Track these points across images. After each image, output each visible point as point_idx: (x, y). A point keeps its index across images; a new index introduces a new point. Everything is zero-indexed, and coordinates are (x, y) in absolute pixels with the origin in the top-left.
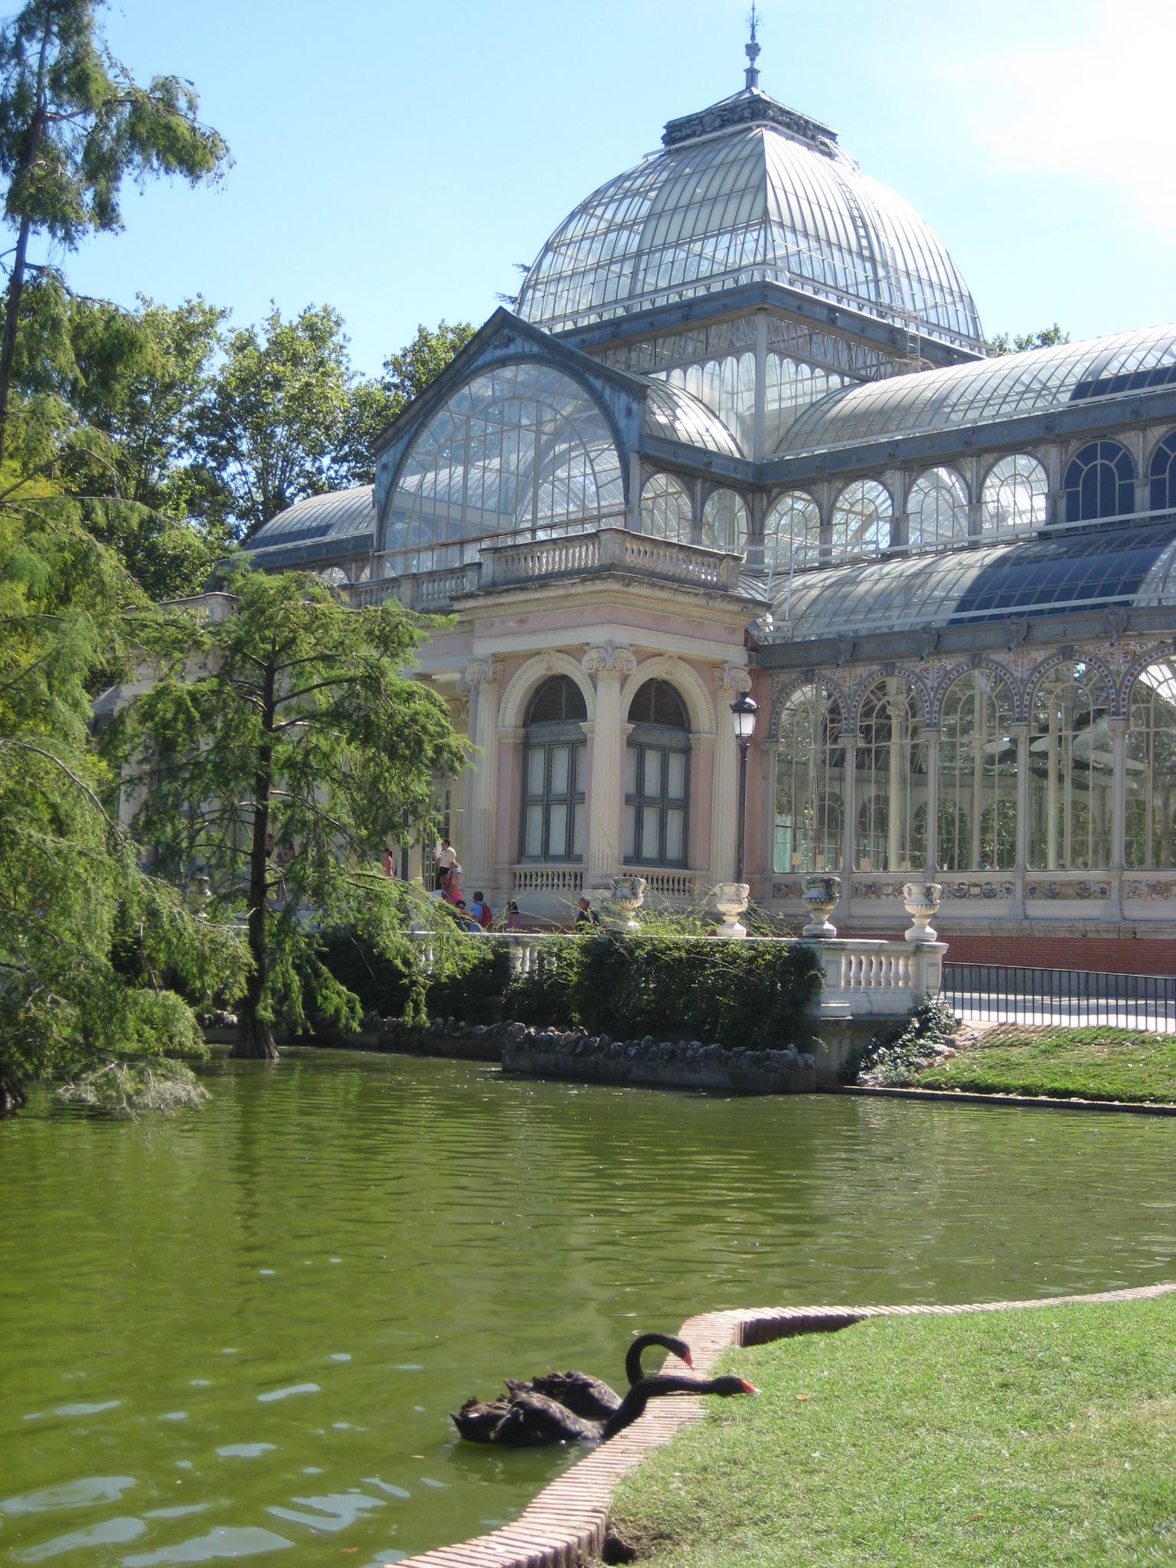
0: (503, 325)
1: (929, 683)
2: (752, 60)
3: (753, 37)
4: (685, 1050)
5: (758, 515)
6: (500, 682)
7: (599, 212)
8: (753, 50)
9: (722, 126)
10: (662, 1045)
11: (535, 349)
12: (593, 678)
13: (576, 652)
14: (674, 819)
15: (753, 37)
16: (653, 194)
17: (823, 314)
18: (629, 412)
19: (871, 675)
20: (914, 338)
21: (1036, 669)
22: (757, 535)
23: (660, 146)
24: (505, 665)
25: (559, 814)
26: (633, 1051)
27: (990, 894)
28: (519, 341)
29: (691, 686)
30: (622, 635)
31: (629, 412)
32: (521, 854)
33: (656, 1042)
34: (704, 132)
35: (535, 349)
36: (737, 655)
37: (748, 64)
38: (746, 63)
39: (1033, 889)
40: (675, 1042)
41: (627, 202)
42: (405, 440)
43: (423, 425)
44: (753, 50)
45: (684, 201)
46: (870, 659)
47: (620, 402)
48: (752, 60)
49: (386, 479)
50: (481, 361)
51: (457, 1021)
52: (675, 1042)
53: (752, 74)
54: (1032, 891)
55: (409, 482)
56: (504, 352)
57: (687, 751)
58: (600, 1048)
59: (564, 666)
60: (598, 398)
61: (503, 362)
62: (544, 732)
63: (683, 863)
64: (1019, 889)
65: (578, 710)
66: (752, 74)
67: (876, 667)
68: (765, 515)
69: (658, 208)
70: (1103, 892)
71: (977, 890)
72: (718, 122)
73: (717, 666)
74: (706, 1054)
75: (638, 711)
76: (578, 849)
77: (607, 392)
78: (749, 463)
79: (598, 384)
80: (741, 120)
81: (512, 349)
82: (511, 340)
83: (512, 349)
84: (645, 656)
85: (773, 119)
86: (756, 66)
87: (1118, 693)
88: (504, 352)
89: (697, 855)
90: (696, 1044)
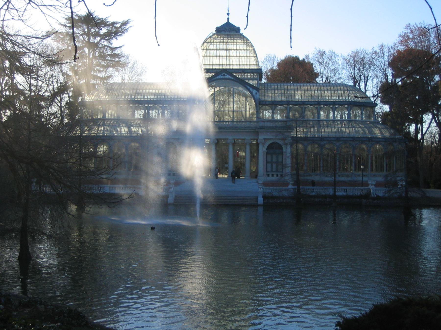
2: (228, 15)
8: (228, 14)
9: (230, 31)
11: (232, 78)
31: (256, 93)
35: (232, 78)
38: (227, 16)
44: (228, 14)
47: (254, 92)
48: (228, 15)
50: (218, 77)
53: (228, 18)
66: (228, 18)
77: (251, 89)
79: (249, 87)
82: (224, 75)
83: (226, 77)
86: (229, 17)
88: (224, 77)
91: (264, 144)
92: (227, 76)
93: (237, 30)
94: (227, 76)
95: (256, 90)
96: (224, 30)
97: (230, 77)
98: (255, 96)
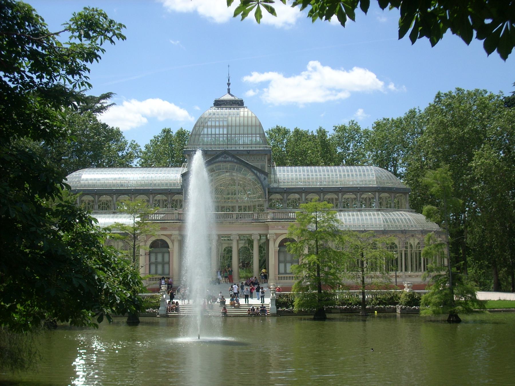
2: (229, 86)
3: (229, 81)
8: (229, 84)
11: (235, 161)
15: (229, 81)
31: (265, 179)
44: (229, 84)
47: (262, 176)
48: (229, 86)
50: (217, 160)
53: (229, 90)
56: (225, 159)
60: (256, 175)
61: (225, 162)
66: (229, 90)
77: (258, 174)
79: (255, 172)
81: (228, 159)
82: (225, 157)
83: (228, 159)
88: (225, 159)
91: (275, 241)
93: (240, 103)
94: (230, 159)
96: (224, 104)
97: (233, 159)
98: (263, 182)
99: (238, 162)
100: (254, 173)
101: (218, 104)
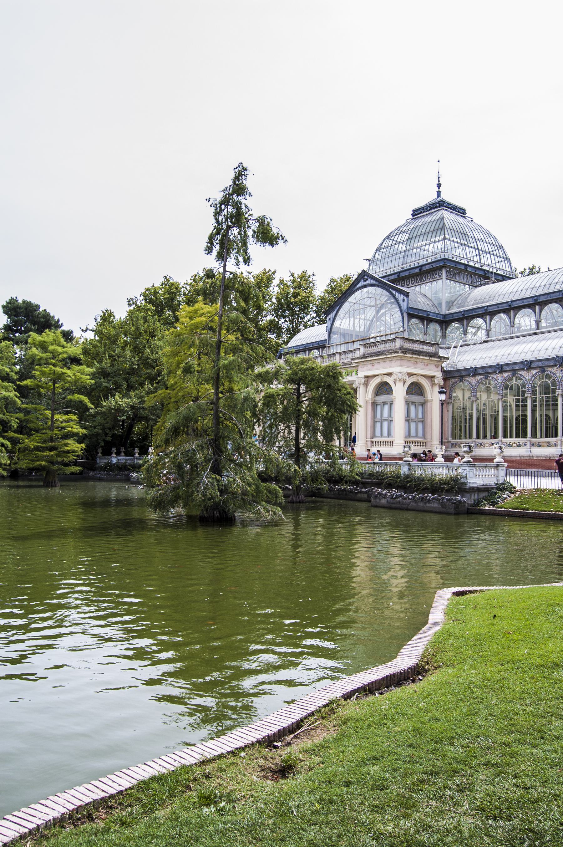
0: (364, 275)
1: (499, 381)
3: (439, 181)
4: (426, 497)
5: (444, 330)
6: (366, 384)
7: (392, 238)
8: (439, 185)
9: (429, 210)
10: (420, 496)
11: (374, 282)
12: (395, 383)
13: (390, 374)
14: (420, 425)
15: (439, 181)
16: (409, 232)
17: (462, 267)
18: (404, 300)
19: (481, 379)
20: (492, 273)
21: (533, 376)
22: (444, 337)
23: (411, 217)
24: (367, 377)
25: (386, 424)
26: (411, 497)
27: (519, 446)
28: (369, 280)
29: (425, 383)
30: (405, 370)
31: (404, 300)
32: (373, 436)
33: (418, 495)
34: (424, 212)
36: (439, 374)
37: (437, 190)
38: (437, 190)
39: (533, 444)
40: (424, 494)
41: (401, 235)
42: (336, 311)
43: (341, 306)
44: (439, 185)
45: (419, 234)
46: (481, 374)
47: (401, 297)
49: (329, 323)
50: (358, 286)
51: (357, 487)
52: (424, 494)
53: (439, 193)
54: (533, 445)
55: (337, 324)
57: (423, 404)
58: (401, 496)
59: (387, 379)
60: (394, 296)
61: (364, 287)
62: (381, 399)
63: (424, 436)
64: (528, 444)
65: (390, 392)
66: (439, 193)
67: (482, 377)
68: (446, 329)
69: (411, 237)
70: (555, 445)
71: (515, 445)
72: (429, 208)
73: (432, 378)
74: (433, 498)
75: (408, 392)
76: (392, 434)
78: (441, 314)
79: (394, 292)
80: (436, 207)
82: (367, 279)
84: (410, 375)
85: (446, 207)
86: (440, 190)
87: (559, 383)
88: (365, 283)
89: (428, 436)
90: (430, 495)
92: (369, 281)
94: (369, 281)
95: (404, 295)
97: (372, 281)
99: (377, 283)
100: (391, 294)
101: (417, 213)
